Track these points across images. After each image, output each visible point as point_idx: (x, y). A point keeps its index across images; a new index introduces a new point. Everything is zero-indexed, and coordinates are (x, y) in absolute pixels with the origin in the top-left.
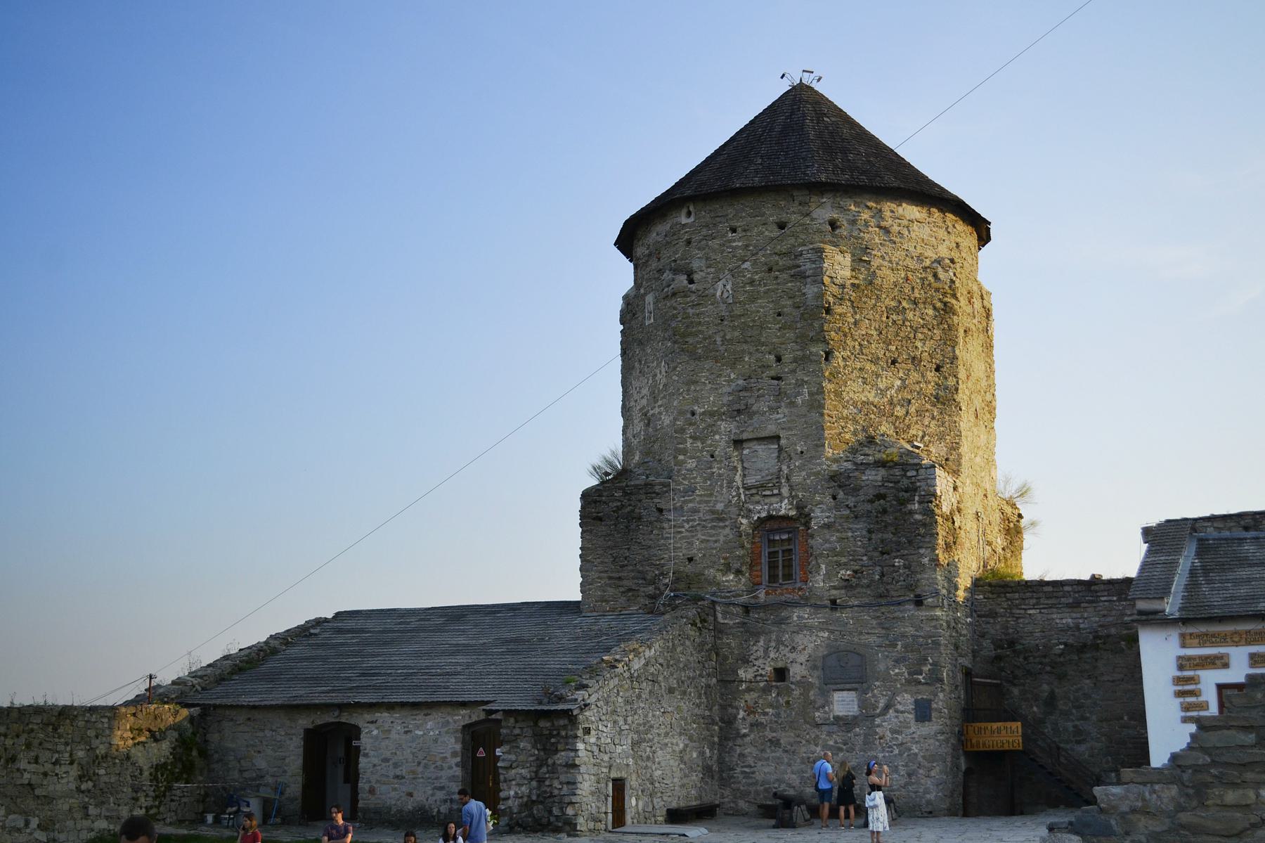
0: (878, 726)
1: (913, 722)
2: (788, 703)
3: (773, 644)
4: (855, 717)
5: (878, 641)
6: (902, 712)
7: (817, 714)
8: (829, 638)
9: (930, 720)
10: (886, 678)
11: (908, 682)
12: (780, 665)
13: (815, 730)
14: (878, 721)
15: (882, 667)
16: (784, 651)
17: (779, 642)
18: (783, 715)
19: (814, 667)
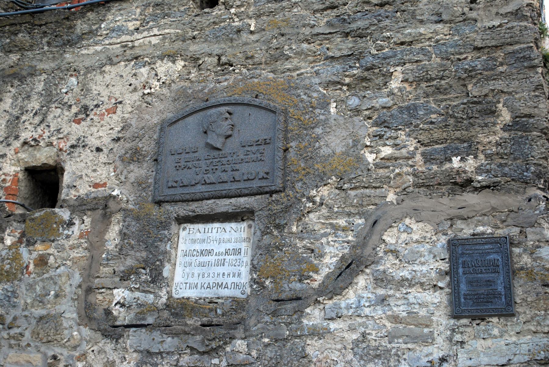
0: (317, 333)
1: (442, 321)
2: (42, 262)
3: (34, 104)
4: (238, 305)
5: (330, 71)
6: (403, 282)
7: (120, 294)
8: (184, 77)
9: (507, 312)
10: (349, 174)
11: (426, 184)
12: (43, 157)
13: (109, 346)
14: (314, 316)
15: (334, 143)
16: (58, 118)
17: (50, 98)
18: (25, 297)
19: (134, 156)
